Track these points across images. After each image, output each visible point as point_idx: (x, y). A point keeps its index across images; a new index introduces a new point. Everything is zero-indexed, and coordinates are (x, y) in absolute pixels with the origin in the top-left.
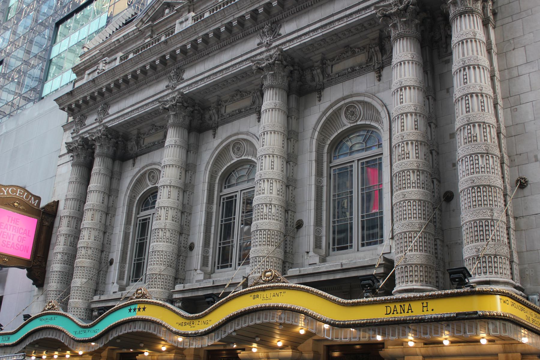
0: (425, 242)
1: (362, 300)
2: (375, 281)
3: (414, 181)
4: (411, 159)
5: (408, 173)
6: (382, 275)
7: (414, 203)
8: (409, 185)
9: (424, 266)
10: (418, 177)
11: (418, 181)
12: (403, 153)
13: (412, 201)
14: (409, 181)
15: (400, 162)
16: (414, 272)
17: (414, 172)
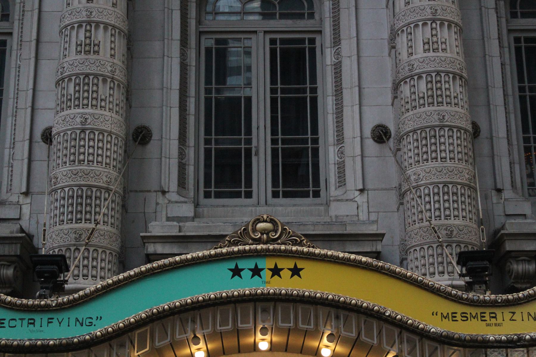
0: (112, 209)
1: (31, 302)
2: (63, 267)
3: (103, 97)
4: (101, 56)
5: (96, 81)
6: (14, 259)
7: (101, 137)
8: (94, 102)
9: (108, 252)
10: (112, 92)
11: (111, 99)
12: (88, 41)
13: (97, 133)
14: (95, 95)
15: (79, 57)
16: (90, 259)
17: (105, 81)
